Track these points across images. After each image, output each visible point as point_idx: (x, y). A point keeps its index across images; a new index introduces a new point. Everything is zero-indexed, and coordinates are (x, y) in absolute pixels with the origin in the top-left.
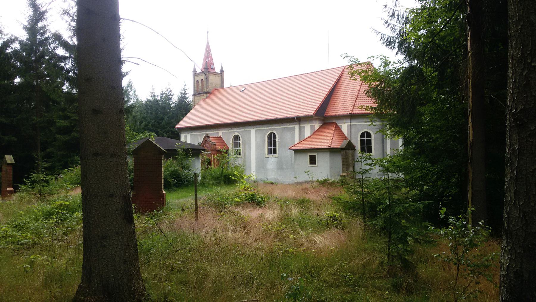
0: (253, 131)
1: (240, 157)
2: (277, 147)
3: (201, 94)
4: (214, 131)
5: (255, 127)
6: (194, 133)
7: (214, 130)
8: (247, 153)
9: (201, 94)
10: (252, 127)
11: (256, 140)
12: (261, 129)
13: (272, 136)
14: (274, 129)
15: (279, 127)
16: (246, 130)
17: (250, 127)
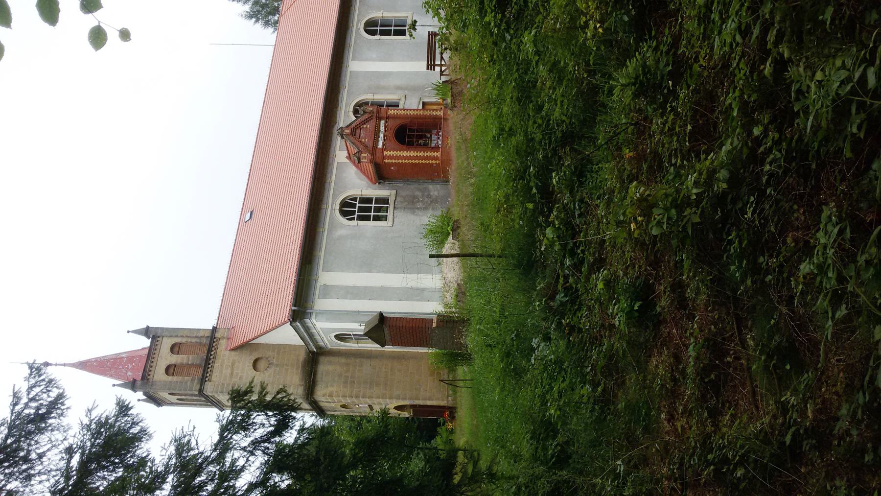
0: (354, 66)
1: (403, 99)
2: (392, 37)
3: (209, 350)
4: (331, 177)
5: (345, 62)
6: (322, 255)
7: (328, 175)
8: (398, 82)
9: (209, 350)
10: (344, 68)
11: (374, 60)
12: (352, 48)
13: (372, 27)
14: (359, 21)
15: (357, 11)
16: (347, 85)
17: (343, 74)
